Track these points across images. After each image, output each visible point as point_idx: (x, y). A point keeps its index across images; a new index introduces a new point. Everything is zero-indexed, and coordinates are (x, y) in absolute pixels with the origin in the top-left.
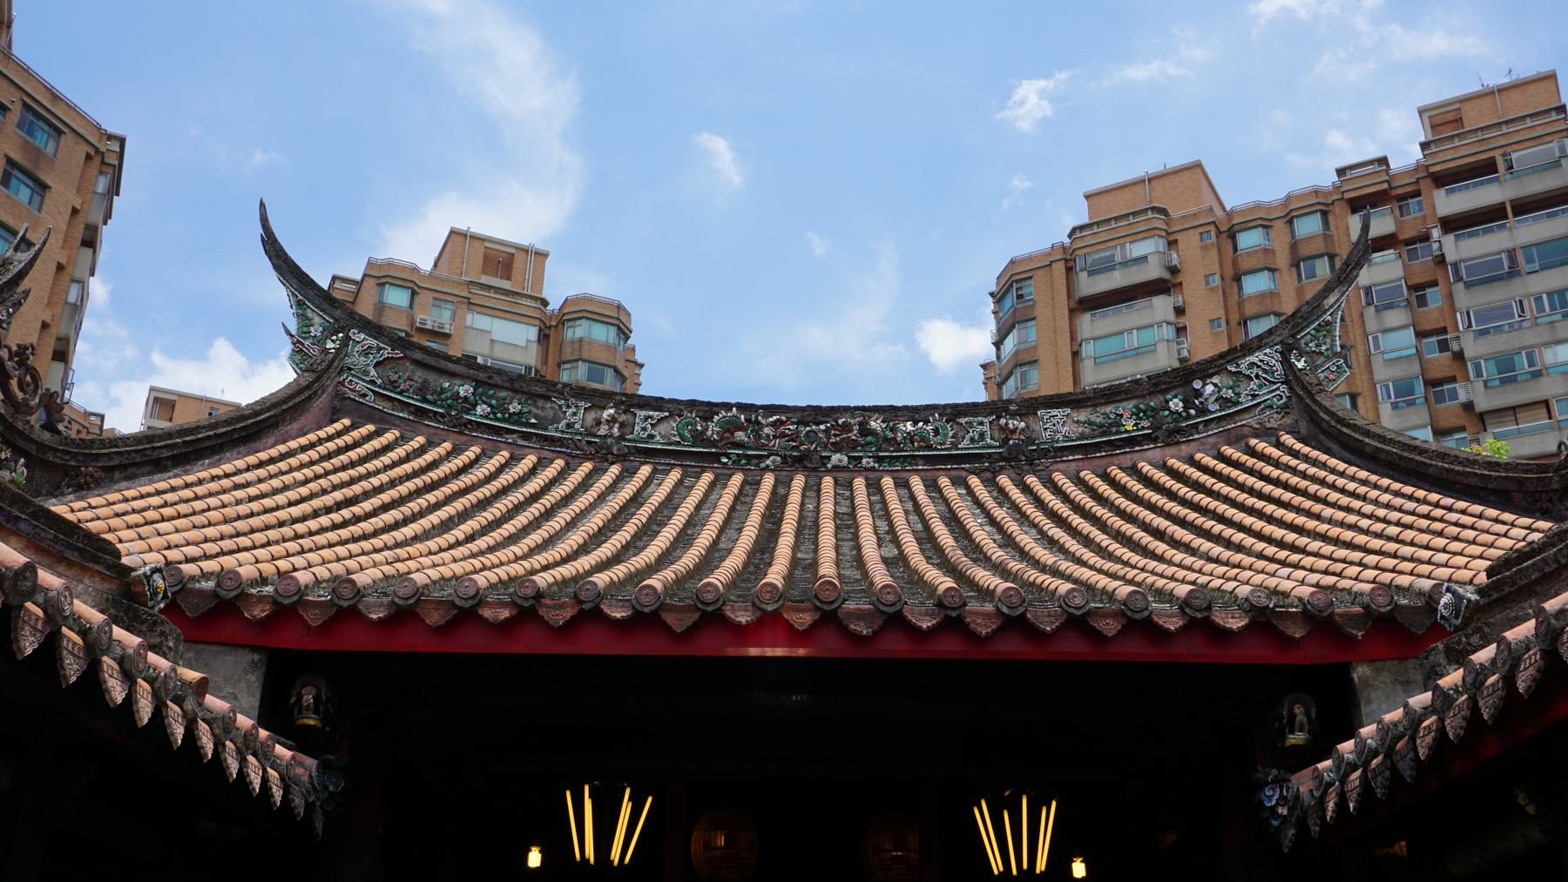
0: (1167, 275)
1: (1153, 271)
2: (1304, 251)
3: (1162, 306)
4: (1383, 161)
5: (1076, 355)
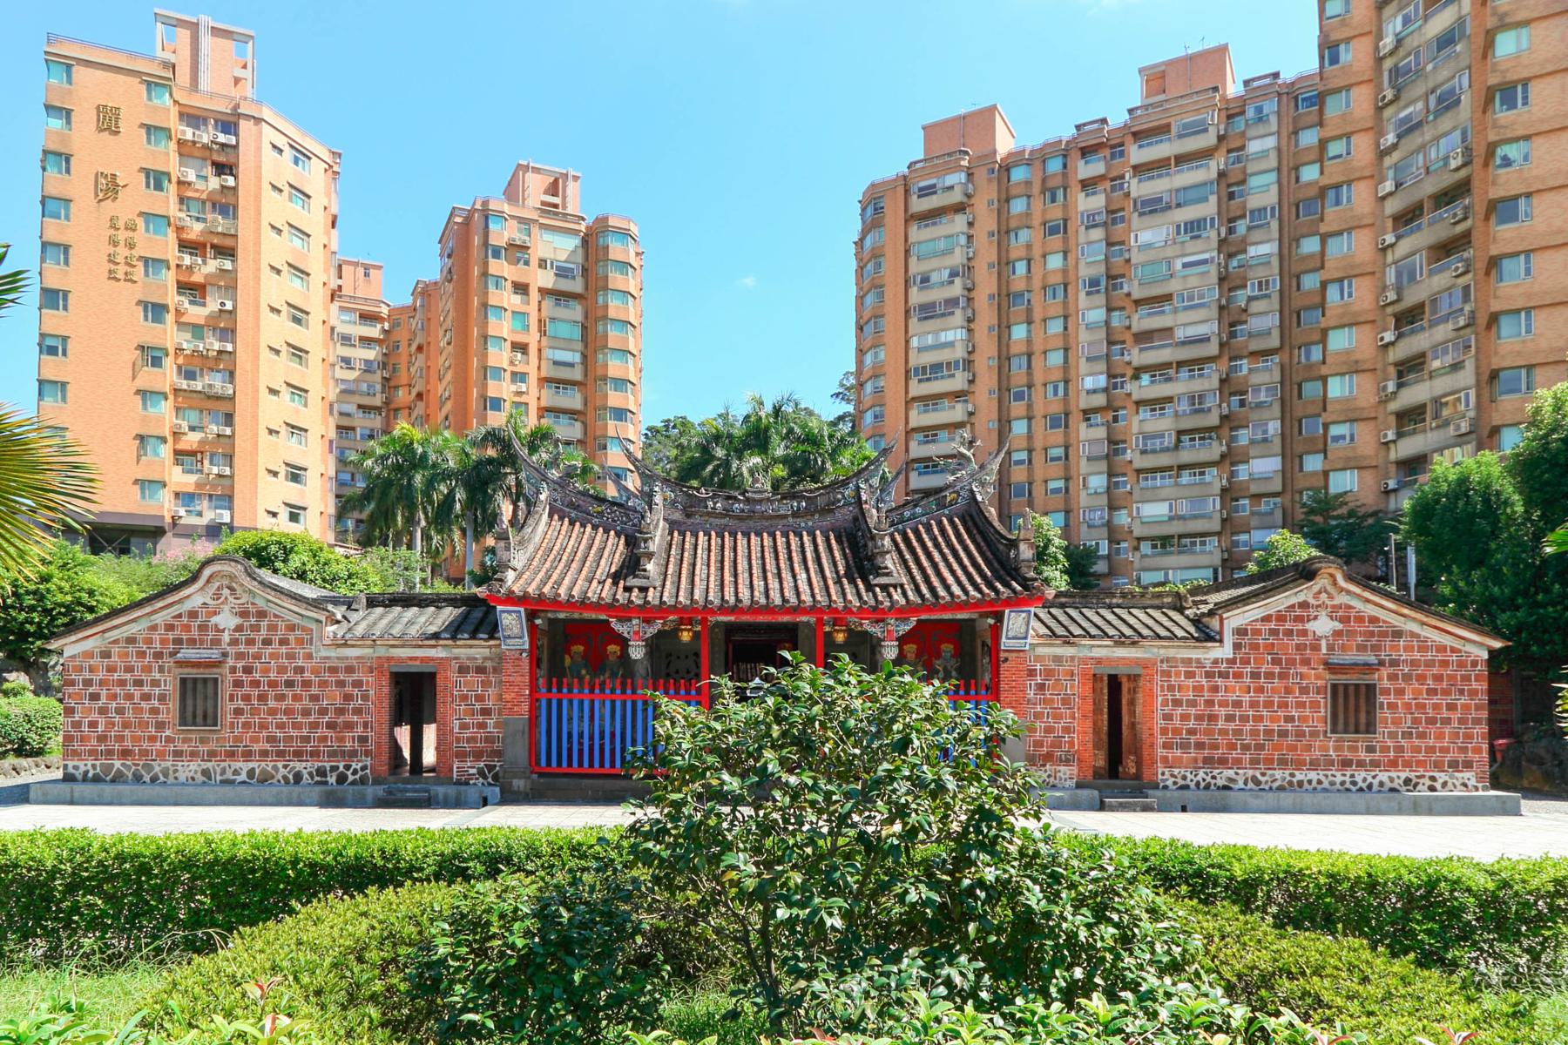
0: (965, 200)
1: (957, 197)
2: (1050, 184)
3: (960, 222)
4: (1104, 121)
5: (907, 252)
